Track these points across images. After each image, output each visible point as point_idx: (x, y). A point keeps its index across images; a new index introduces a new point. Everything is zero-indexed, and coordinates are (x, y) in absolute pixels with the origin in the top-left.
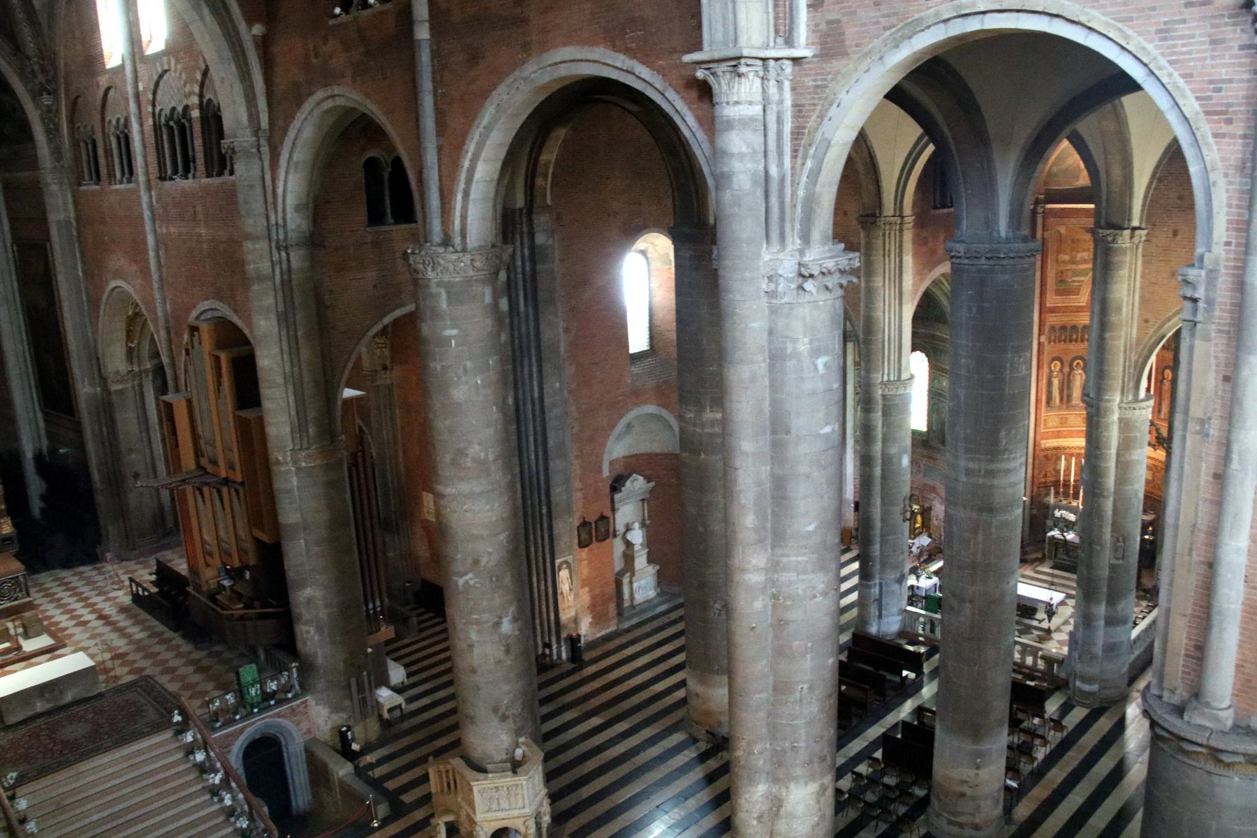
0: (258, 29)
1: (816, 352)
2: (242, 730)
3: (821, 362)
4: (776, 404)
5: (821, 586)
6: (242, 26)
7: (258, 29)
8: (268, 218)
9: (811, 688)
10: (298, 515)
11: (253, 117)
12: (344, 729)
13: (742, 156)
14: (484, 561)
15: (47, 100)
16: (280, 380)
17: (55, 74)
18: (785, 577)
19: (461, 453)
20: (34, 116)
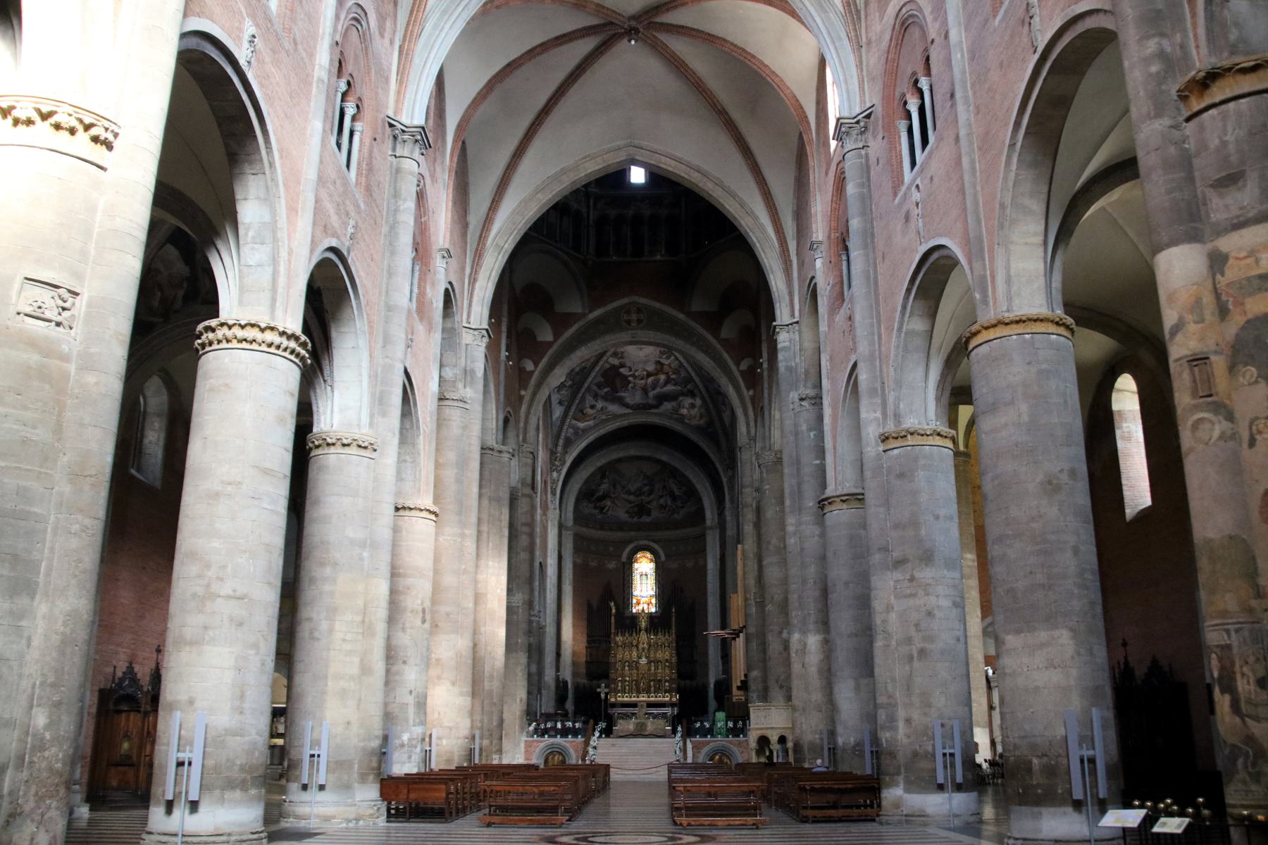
0: (751, 392)
1: (810, 430)
2: (708, 743)
3: (812, 434)
4: (797, 452)
5: (817, 532)
6: (745, 391)
7: (751, 392)
8: (752, 477)
9: (815, 583)
10: (754, 629)
11: (748, 432)
12: (740, 724)
13: (781, 361)
14: (776, 597)
15: (730, 472)
16: (751, 556)
18: (803, 527)
19: (769, 543)
20: (725, 480)
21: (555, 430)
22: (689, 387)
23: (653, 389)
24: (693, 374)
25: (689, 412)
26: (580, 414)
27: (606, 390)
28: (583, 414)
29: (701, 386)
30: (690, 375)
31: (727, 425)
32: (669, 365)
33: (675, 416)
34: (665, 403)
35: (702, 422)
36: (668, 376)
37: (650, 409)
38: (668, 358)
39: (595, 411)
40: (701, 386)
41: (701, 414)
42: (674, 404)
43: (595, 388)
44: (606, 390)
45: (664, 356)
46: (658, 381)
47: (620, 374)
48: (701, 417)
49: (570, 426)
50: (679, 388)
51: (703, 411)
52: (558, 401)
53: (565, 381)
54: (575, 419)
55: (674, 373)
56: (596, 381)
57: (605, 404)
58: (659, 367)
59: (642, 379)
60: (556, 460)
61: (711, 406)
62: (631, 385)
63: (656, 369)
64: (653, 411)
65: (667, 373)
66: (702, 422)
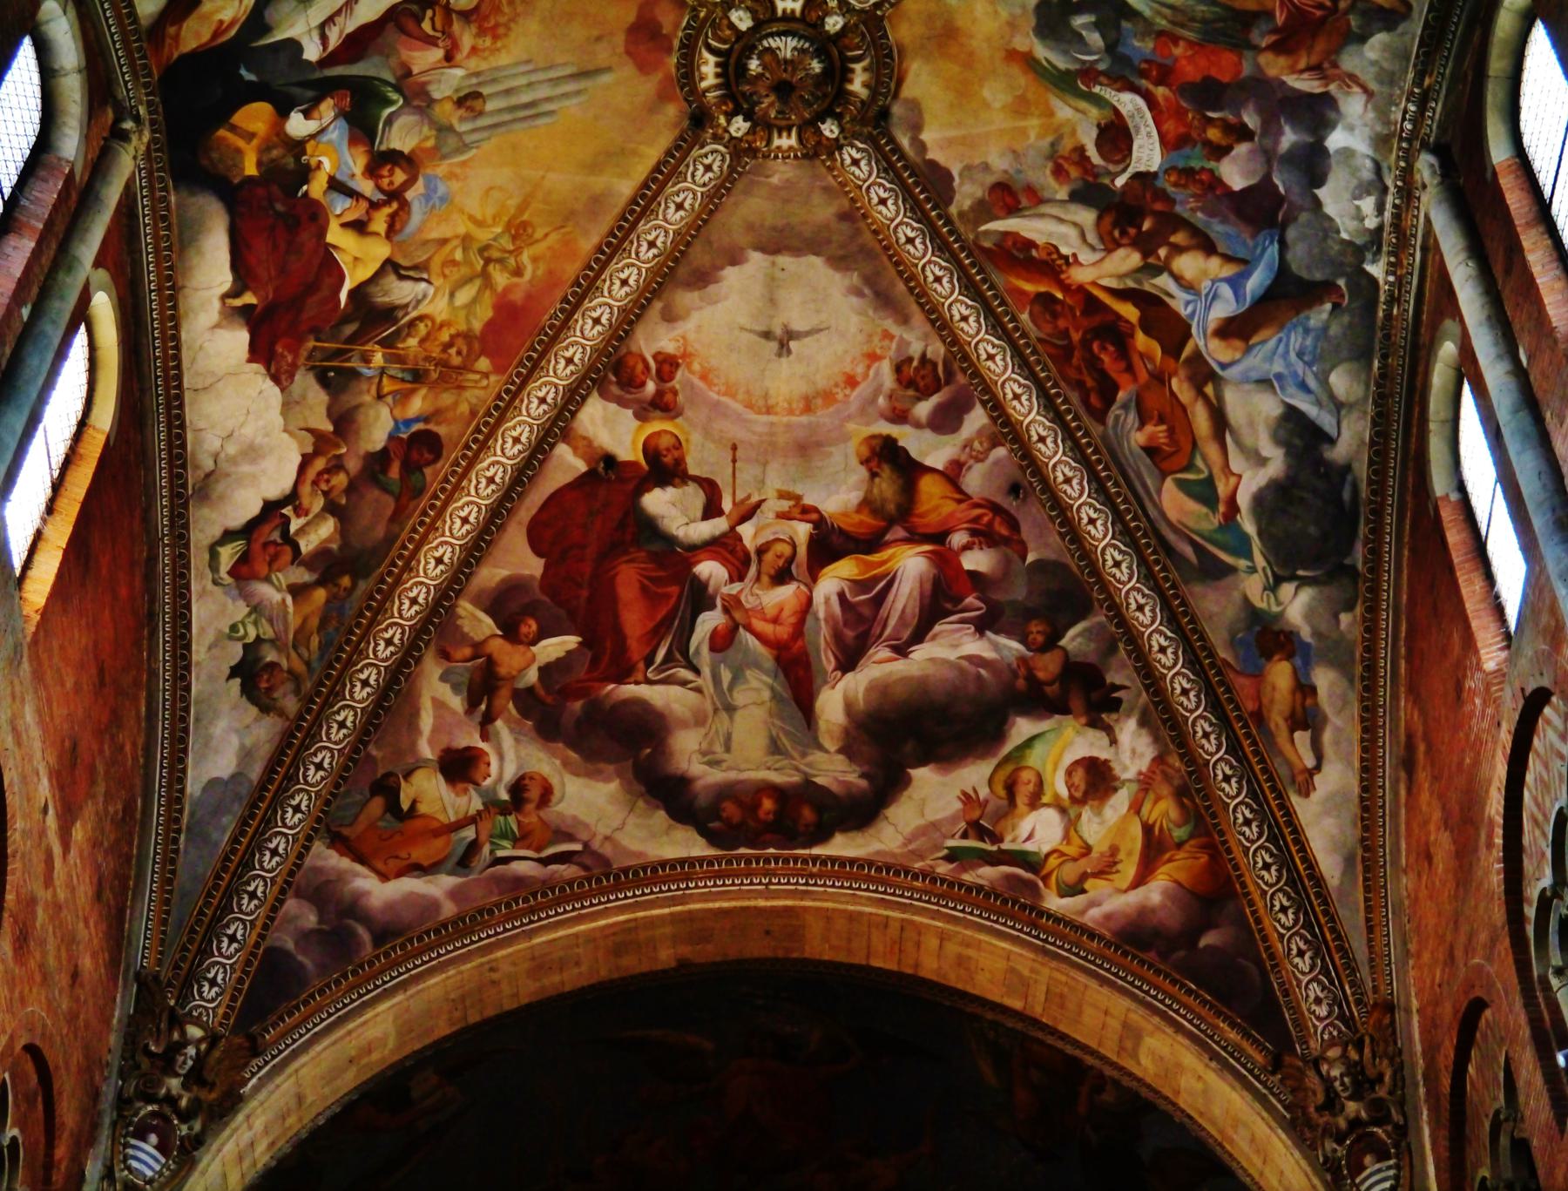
17: (1399, 1070)
21: (197, 863)
22: (1074, 639)
23: (849, 660)
24: (1100, 534)
25: (1071, 825)
26: (377, 805)
27: (556, 647)
28: (393, 806)
29: (1146, 617)
30: (1087, 555)
31: (1330, 866)
32: (953, 475)
33: (986, 874)
34: (924, 776)
35: (1154, 893)
36: (944, 561)
37: (823, 836)
38: (945, 421)
39: (477, 804)
40: (1146, 617)
41: (1147, 829)
42: (976, 775)
43: (478, 623)
44: (556, 647)
45: (923, 409)
46: (877, 589)
47: (649, 528)
48: (1154, 849)
49: (293, 882)
50: (1013, 646)
51: (1163, 810)
52: (236, 652)
53: (292, 498)
54: (340, 843)
55: (983, 536)
56: (490, 575)
57: (543, 762)
58: (887, 487)
59: (782, 576)
60: (167, 1062)
61: (1211, 747)
62: (709, 621)
63: (866, 504)
64: (841, 846)
65: (938, 537)
66: (1154, 893)
